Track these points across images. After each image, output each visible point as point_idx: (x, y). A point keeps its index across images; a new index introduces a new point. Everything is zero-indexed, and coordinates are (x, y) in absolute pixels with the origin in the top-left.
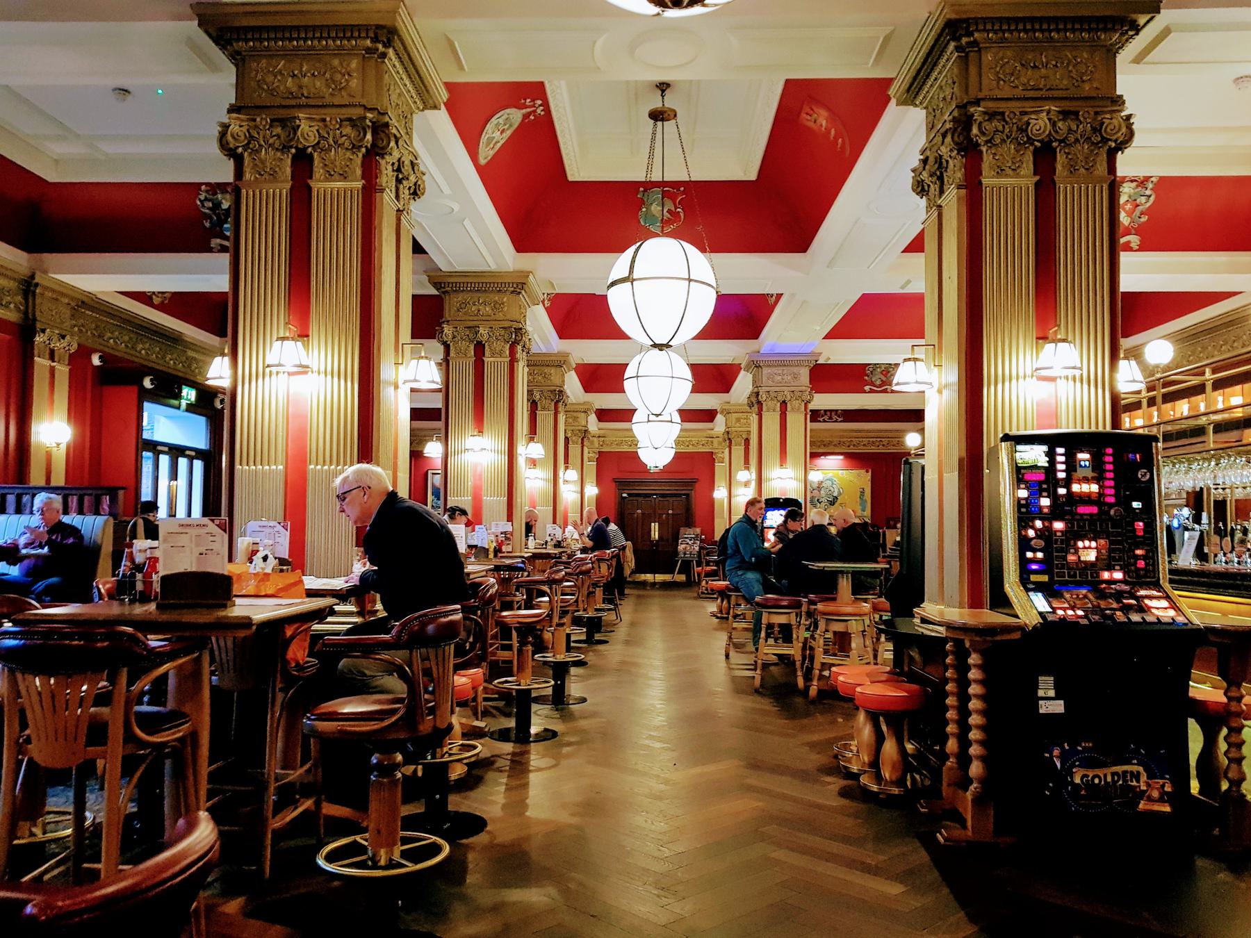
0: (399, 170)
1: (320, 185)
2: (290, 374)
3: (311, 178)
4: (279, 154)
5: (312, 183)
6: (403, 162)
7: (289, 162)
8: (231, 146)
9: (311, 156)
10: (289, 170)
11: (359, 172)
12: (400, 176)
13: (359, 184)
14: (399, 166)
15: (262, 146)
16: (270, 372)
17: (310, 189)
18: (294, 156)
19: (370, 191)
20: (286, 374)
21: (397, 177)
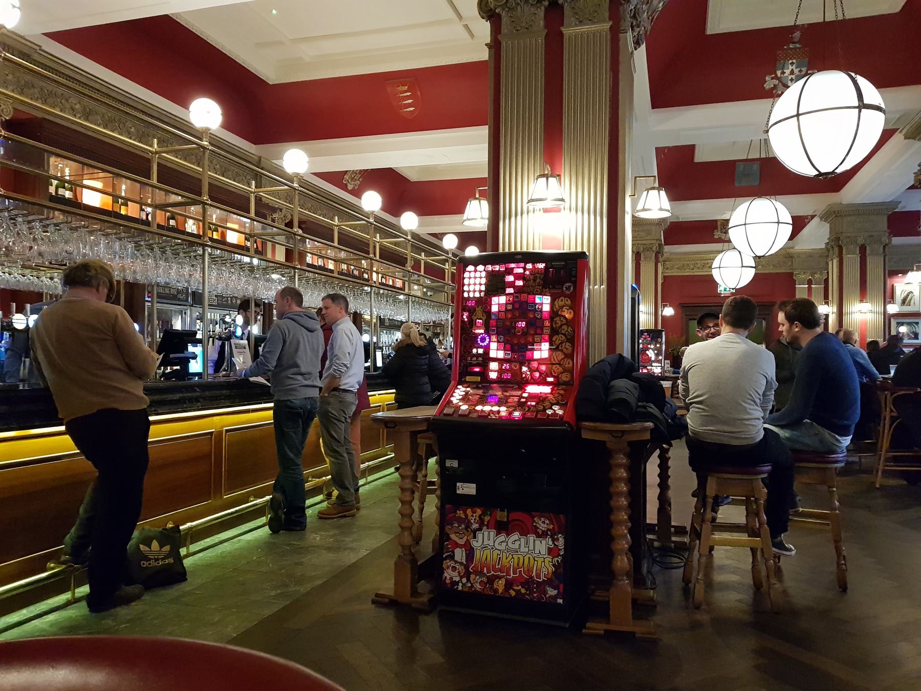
0: (634, 17)
1: (570, 30)
2: (546, 211)
3: (563, 26)
4: (533, 10)
5: (563, 29)
6: (638, 10)
7: (542, 14)
8: (492, 6)
9: (562, 7)
10: (542, 23)
11: (607, 14)
12: (634, 23)
13: (607, 26)
14: (635, 14)
15: (518, 3)
16: (528, 207)
17: (561, 34)
18: (546, 9)
19: (615, 33)
20: (542, 211)
21: (632, 24)
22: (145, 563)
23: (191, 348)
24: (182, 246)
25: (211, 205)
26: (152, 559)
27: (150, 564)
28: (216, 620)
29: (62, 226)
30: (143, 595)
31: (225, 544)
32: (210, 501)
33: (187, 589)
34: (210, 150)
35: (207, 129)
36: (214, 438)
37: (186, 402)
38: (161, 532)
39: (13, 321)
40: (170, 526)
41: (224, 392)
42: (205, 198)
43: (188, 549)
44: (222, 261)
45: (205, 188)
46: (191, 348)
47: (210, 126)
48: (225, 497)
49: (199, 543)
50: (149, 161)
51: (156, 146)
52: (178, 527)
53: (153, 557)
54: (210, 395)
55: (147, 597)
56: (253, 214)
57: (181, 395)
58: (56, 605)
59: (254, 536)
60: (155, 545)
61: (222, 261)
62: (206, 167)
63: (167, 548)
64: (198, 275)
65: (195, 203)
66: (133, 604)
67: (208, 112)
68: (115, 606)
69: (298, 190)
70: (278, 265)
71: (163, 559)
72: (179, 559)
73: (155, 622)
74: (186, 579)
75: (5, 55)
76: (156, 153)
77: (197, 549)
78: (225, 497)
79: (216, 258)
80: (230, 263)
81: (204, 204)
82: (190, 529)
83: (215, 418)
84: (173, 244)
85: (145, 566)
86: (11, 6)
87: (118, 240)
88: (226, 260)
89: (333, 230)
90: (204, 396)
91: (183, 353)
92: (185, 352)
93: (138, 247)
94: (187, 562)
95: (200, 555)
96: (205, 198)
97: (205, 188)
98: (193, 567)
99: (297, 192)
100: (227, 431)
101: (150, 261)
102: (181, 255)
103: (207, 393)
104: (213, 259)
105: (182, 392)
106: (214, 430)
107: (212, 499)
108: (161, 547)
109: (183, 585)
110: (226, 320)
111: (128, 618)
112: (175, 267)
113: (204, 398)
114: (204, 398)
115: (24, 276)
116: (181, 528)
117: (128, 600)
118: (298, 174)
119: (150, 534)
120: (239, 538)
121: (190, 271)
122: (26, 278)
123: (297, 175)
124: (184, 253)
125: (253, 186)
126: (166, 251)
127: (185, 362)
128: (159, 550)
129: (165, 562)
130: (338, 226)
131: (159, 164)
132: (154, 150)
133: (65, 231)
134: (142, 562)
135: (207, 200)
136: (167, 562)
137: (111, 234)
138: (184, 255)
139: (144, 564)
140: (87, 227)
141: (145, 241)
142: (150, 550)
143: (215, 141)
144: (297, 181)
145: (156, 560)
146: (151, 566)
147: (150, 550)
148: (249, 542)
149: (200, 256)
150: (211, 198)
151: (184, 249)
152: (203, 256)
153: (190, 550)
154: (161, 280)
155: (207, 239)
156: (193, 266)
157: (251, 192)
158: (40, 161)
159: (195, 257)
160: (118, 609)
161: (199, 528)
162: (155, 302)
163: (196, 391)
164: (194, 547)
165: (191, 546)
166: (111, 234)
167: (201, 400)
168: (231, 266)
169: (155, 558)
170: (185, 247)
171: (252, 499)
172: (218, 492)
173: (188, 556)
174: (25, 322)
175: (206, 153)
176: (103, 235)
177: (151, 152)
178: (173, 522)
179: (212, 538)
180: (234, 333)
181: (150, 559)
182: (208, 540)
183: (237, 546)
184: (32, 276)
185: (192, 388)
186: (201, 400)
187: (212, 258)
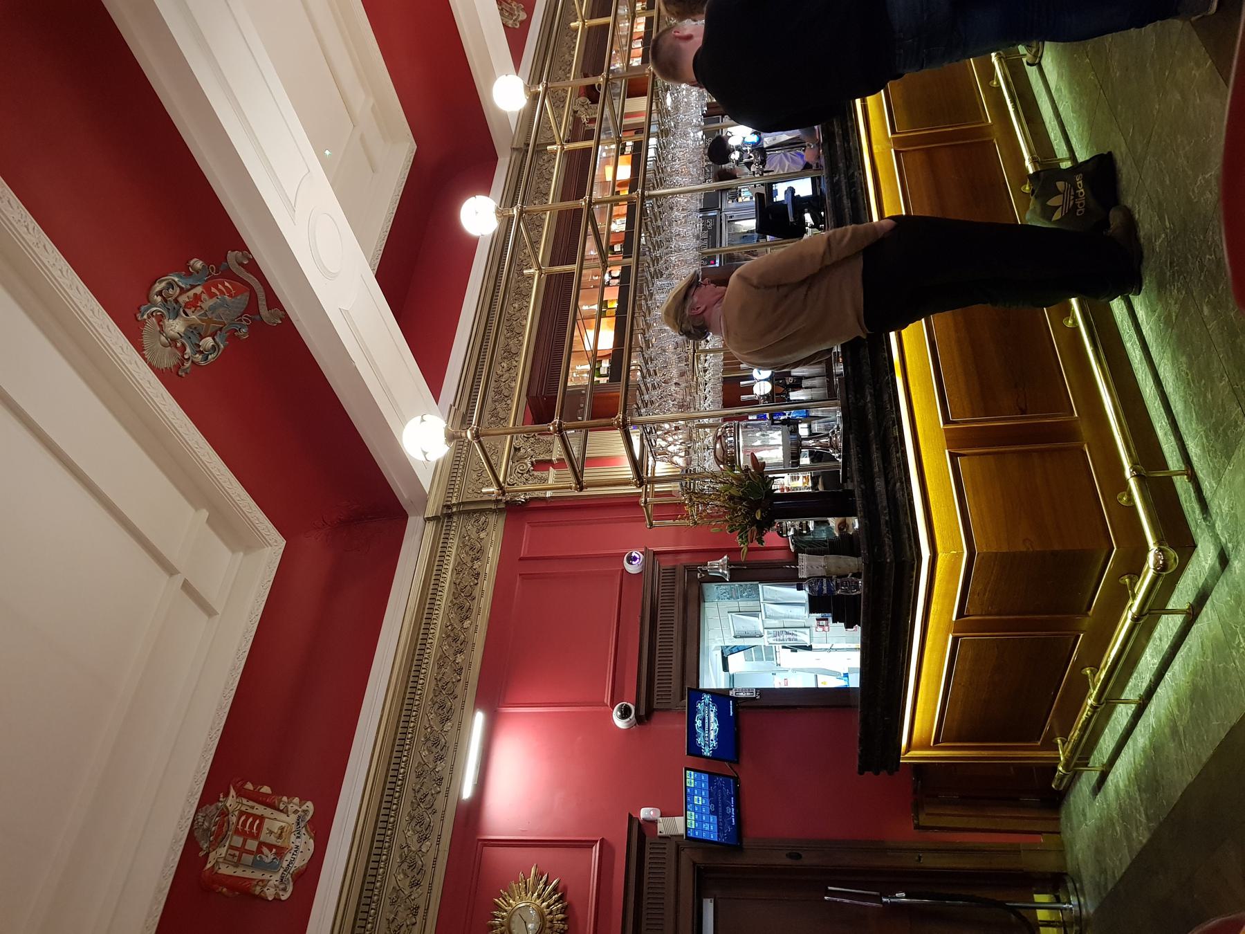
22: (1078, 210)
23: (780, 197)
24: (649, 223)
25: (591, 195)
26: (1075, 201)
27: (1081, 205)
28: (1178, 97)
29: (646, 356)
30: (1125, 207)
31: (1061, 109)
32: (995, 141)
33: (1124, 148)
34: (522, 204)
35: (497, 212)
36: (902, 147)
37: (854, 190)
38: (1036, 197)
39: (762, 394)
40: (1027, 188)
41: (838, 143)
42: (583, 204)
43: (1062, 160)
44: (659, 173)
45: (570, 204)
46: (780, 197)
47: (493, 210)
48: (990, 121)
49: (1055, 147)
50: (550, 277)
51: (532, 271)
52: (1030, 176)
53: (1071, 203)
54: (844, 161)
55: (1128, 201)
56: (591, 143)
57: (845, 197)
58: (1125, 310)
59: (1051, 69)
60: (1054, 201)
61: (659, 173)
62: (544, 207)
63: (1060, 185)
64: (682, 200)
65: (591, 217)
66: (1137, 216)
67: (477, 213)
68: (1137, 239)
69: (547, 84)
70: (654, 97)
71: (1076, 189)
72: (1077, 167)
73: (1168, 182)
74: (1110, 153)
75: (475, 425)
76: (540, 269)
77: (1065, 148)
78: (990, 121)
79: (657, 180)
80: (660, 161)
81: (590, 203)
82: (1034, 161)
83: (875, 150)
84: (648, 234)
85: (1083, 210)
86: (424, 422)
87: (654, 297)
88: (658, 167)
89: (590, 28)
90: (845, 169)
91: (786, 205)
92: (785, 203)
93: (658, 274)
94: (1082, 156)
95: (1074, 141)
96: (583, 204)
97: (570, 204)
98: (1091, 147)
99: (549, 85)
100: (893, 132)
101: (673, 259)
102: (659, 223)
103: (841, 165)
104: (661, 183)
105: (841, 198)
106: (893, 150)
107: (992, 138)
108: (1058, 193)
109: (1118, 157)
110: (737, 159)
111: (1157, 218)
112: (675, 229)
113: (848, 167)
114: (848, 167)
115: (706, 398)
116: (1031, 171)
117: (1131, 224)
118: (525, 86)
119: (1038, 210)
120: (1053, 91)
121: (678, 210)
122: (708, 396)
123: (527, 88)
124: (656, 220)
125: (554, 147)
126: (657, 241)
127: (800, 204)
128: (1062, 195)
129: (1080, 184)
130: (584, 21)
131: (552, 264)
132: (537, 272)
133: (652, 352)
134: (1078, 214)
135: (585, 200)
136: (1081, 182)
137: (647, 305)
138: (659, 221)
139: (1080, 212)
140: (644, 331)
141: (649, 267)
142: (1061, 208)
143: (509, 199)
144: (535, 87)
145: (1076, 196)
146: (1084, 201)
147: (1061, 208)
148: (1060, 76)
149: (657, 200)
150: (580, 195)
151: (651, 221)
152: (657, 197)
153: (1064, 157)
154: (694, 243)
155: (634, 194)
156: (672, 208)
157: (563, 149)
158: (577, 394)
159: (659, 207)
160: (1142, 234)
161: (1033, 147)
162: (721, 249)
163: (839, 180)
164: (1061, 151)
165: (1059, 157)
166: (647, 305)
167: (851, 171)
168: (664, 160)
169: (1074, 199)
170: (649, 219)
171: (995, 83)
172: (982, 131)
173: (1073, 156)
174: (762, 382)
175: (527, 209)
176: (650, 314)
177: (540, 276)
178: (1022, 185)
179: (1050, 130)
180: (754, 145)
181: (1075, 205)
182: (1052, 136)
183: (1065, 92)
184: (705, 390)
185: (835, 188)
186: (851, 171)
187: (658, 186)
